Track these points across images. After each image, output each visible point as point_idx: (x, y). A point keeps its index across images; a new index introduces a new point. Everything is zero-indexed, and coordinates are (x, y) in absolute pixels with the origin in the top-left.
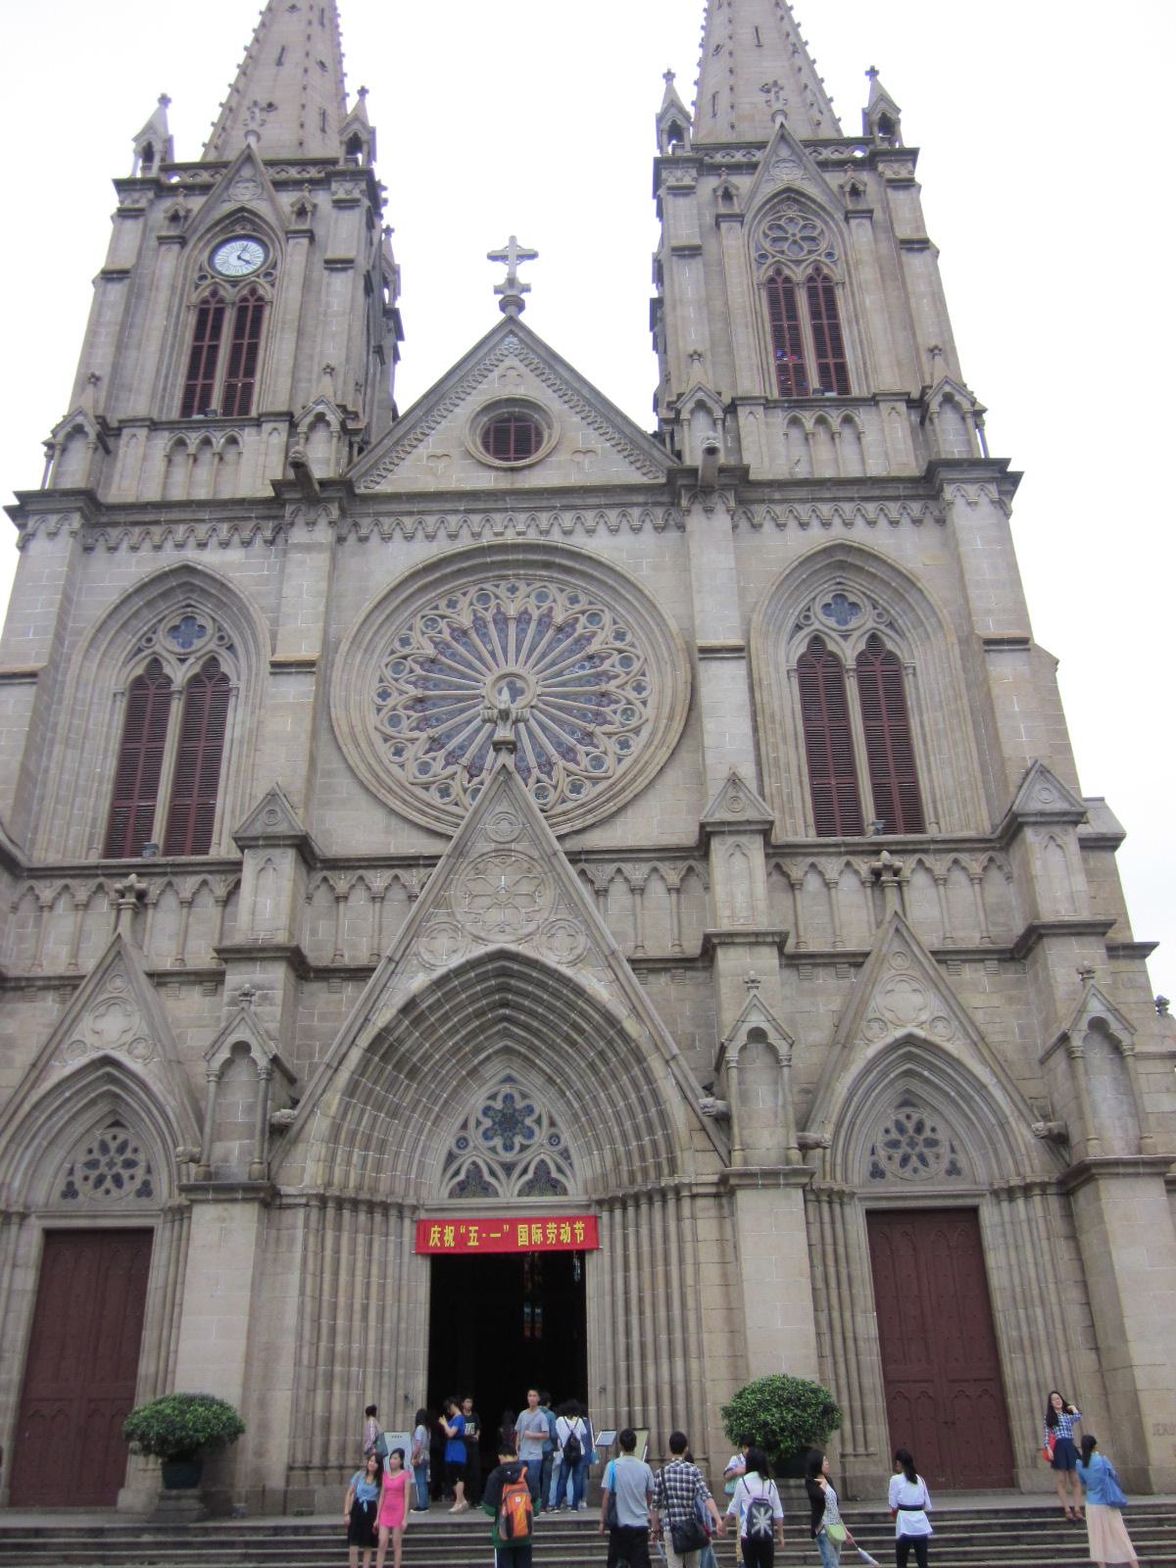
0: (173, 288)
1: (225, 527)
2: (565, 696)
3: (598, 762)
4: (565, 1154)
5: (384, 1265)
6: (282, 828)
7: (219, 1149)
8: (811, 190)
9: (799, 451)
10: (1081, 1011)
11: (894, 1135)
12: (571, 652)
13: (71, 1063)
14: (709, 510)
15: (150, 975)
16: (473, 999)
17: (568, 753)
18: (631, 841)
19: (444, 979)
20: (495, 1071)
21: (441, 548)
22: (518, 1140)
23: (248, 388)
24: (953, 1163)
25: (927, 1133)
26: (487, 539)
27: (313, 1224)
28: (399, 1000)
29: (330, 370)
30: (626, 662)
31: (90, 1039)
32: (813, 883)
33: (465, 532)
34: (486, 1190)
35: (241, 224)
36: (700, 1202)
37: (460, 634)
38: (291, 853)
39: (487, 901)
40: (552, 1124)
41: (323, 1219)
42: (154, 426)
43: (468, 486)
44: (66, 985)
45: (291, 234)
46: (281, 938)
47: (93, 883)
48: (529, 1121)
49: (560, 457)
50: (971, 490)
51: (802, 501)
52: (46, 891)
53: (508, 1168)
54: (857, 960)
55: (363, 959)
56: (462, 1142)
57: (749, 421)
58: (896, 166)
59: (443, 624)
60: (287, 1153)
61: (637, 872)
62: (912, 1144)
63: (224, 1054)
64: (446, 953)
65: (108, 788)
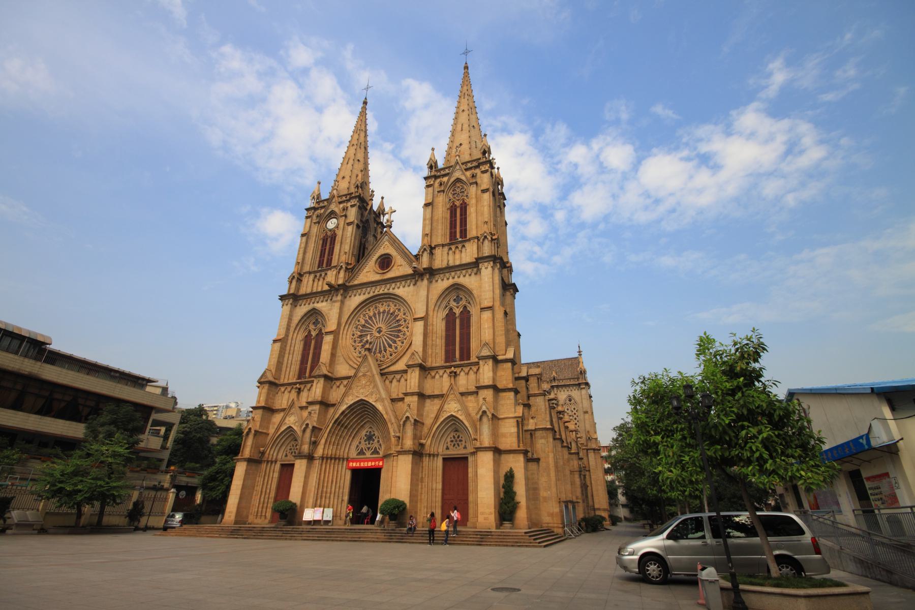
0: (316, 235)
1: (322, 297)
2: (390, 331)
3: (396, 348)
4: (380, 445)
5: (337, 471)
6: (321, 373)
7: (303, 447)
8: (463, 178)
9: (451, 257)
10: (480, 409)
11: (453, 439)
13: (283, 428)
14: (422, 280)
15: (300, 407)
16: (359, 410)
17: (390, 346)
18: (399, 369)
20: (368, 425)
21: (367, 296)
22: (371, 442)
23: (332, 258)
24: (465, 446)
25: (460, 438)
26: (376, 293)
27: (320, 463)
28: (340, 412)
29: (346, 253)
30: (405, 321)
31: (288, 423)
32: (437, 376)
33: (371, 292)
34: (364, 454)
35: (332, 214)
36: (395, 458)
37: (370, 318)
38: (323, 379)
39: (360, 387)
41: (322, 462)
42: (310, 273)
43: (373, 280)
44: (283, 410)
45: (342, 216)
46: (320, 399)
47: (291, 387)
49: (395, 268)
50: (486, 264)
51: (448, 272)
52: (283, 389)
53: (369, 448)
54: (442, 396)
56: (360, 443)
57: (438, 252)
59: (367, 315)
60: (316, 448)
61: (398, 376)
62: (456, 441)
63: (304, 426)
64: (350, 400)
65: (299, 363)
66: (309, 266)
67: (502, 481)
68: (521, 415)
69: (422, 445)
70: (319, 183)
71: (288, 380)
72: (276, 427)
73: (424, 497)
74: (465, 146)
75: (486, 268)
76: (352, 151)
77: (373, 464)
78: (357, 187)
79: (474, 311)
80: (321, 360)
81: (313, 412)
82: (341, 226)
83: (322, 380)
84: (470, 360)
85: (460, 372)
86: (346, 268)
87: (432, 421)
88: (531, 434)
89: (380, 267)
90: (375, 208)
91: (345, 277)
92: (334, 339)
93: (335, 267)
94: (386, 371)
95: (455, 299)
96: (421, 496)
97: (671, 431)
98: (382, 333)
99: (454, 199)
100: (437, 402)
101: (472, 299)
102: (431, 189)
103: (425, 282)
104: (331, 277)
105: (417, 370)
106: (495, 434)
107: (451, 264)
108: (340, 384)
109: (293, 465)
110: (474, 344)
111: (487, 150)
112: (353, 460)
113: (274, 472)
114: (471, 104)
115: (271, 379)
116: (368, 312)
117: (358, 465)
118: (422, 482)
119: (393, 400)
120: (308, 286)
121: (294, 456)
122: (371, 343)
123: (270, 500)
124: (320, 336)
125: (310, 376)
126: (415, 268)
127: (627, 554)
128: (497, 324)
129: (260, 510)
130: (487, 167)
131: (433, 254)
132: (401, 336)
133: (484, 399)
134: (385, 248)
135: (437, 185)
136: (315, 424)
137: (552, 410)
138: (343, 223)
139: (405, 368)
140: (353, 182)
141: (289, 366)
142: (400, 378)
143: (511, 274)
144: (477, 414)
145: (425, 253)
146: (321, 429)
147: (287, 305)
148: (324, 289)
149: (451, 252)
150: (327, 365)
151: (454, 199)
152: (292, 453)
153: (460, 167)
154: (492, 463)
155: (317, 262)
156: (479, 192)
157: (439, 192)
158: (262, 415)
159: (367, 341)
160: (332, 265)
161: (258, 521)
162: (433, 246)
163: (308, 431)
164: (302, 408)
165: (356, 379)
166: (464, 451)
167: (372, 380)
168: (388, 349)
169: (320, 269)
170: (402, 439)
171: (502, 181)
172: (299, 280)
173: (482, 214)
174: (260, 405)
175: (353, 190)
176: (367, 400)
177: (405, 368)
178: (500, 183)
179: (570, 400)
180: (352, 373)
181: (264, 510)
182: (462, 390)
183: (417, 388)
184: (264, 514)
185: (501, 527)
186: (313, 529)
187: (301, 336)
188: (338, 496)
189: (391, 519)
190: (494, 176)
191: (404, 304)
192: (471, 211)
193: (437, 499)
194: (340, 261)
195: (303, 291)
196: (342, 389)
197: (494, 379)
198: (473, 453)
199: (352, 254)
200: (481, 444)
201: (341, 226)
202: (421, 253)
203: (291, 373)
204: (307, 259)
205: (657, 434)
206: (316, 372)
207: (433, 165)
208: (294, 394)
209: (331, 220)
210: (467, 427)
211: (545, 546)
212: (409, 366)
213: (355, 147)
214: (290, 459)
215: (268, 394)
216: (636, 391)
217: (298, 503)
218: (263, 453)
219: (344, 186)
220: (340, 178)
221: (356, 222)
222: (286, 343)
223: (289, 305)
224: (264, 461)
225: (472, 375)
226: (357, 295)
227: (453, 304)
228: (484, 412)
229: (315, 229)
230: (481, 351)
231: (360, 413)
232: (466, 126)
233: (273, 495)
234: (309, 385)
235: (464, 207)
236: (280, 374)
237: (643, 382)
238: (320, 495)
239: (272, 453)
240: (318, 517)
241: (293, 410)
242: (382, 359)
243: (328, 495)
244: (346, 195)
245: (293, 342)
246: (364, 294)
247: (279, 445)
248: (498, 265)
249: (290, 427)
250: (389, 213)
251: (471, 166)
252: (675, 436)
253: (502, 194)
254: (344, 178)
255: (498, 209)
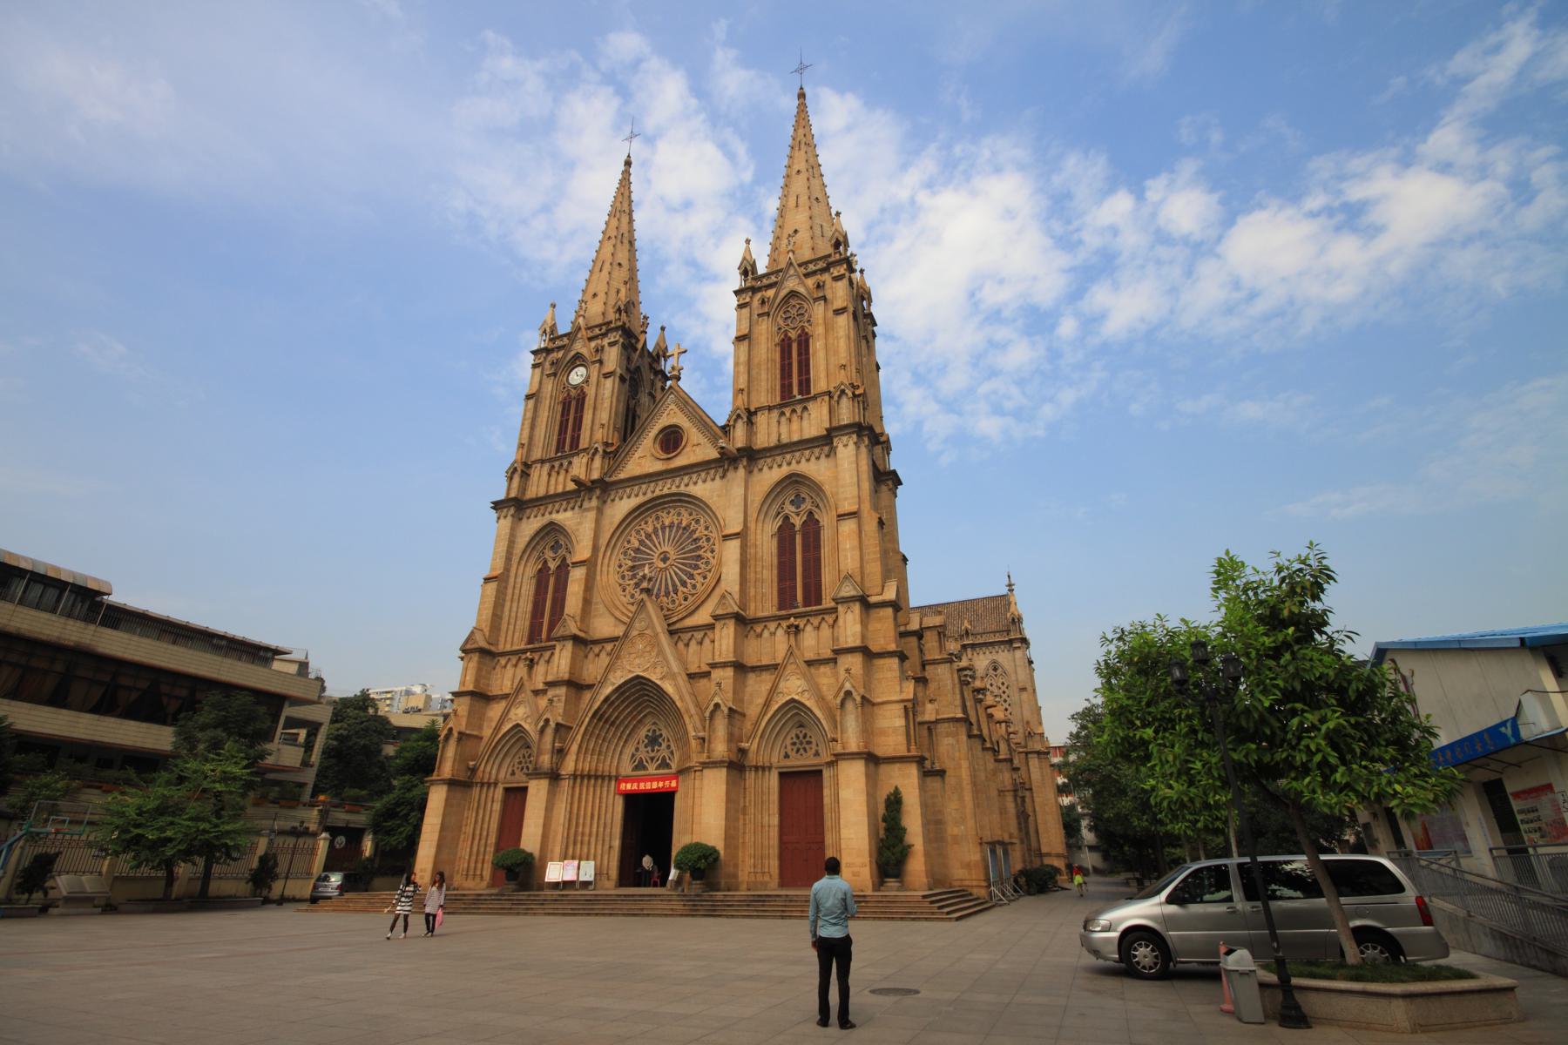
0: (551, 396)
2: (683, 559)
3: (694, 587)
4: (672, 753)
5: (601, 798)
6: (567, 633)
7: (541, 758)
8: (802, 290)
9: (784, 429)
12: (688, 538)
15: (533, 691)
16: (633, 694)
17: (684, 584)
18: (701, 622)
19: (620, 687)
20: (649, 720)
21: (641, 499)
22: (656, 748)
23: (579, 436)
25: (808, 739)
26: (658, 493)
28: (602, 698)
29: (603, 425)
30: (708, 540)
31: (514, 718)
32: (766, 634)
33: (649, 491)
34: (645, 768)
35: (578, 360)
36: (698, 773)
37: (648, 536)
38: (571, 642)
39: (633, 656)
40: (668, 741)
41: (574, 783)
42: (542, 461)
44: (505, 697)
46: (566, 677)
48: (660, 740)
49: (688, 449)
50: (845, 439)
52: (503, 661)
53: (652, 759)
54: (774, 667)
55: (591, 683)
56: (637, 749)
57: (761, 419)
58: (838, 268)
59: (642, 532)
61: (699, 635)
62: (801, 743)
63: (541, 723)
64: (618, 678)
65: (528, 616)
66: (540, 450)
67: (882, 810)
68: (911, 696)
69: (743, 752)
70: (554, 306)
71: (512, 645)
72: (494, 725)
73: (750, 838)
74: (804, 235)
75: (846, 446)
76: (609, 248)
77: (661, 784)
78: (619, 310)
79: (826, 520)
80: (567, 610)
81: (555, 699)
82: (594, 379)
83: (569, 645)
84: (821, 604)
85: (805, 625)
86: (604, 451)
87: (759, 710)
88: (929, 728)
89: (662, 450)
90: (651, 347)
91: (602, 468)
92: (587, 574)
93: (584, 450)
94: (678, 626)
95: (792, 501)
96: (744, 838)
97: (1171, 720)
98: (668, 563)
99: (787, 328)
100: (767, 679)
101: (821, 499)
102: (746, 311)
103: (741, 472)
104: (579, 467)
105: (731, 624)
106: (867, 730)
107: (785, 439)
108: (601, 651)
109: (525, 789)
110: (827, 577)
111: (841, 239)
112: (627, 779)
113: (493, 801)
114: (811, 160)
115: (483, 644)
116: (643, 526)
117: (635, 787)
118: (744, 814)
119: (691, 676)
120: (540, 483)
121: (527, 775)
122: (650, 580)
123: (488, 849)
124: (564, 569)
125: (549, 639)
126: (722, 448)
127: (1099, 929)
128: (866, 542)
129: (472, 865)
130: (842, 269)
131: (752, 423)
132: (703, 566)
133: (847, 670)
134: (670, 415)
135: (756, 302)
136: (560, 720)
137: (965, 687)
138: (596, 373)
139: (711, 621)
140: (612, 302)
141: (512, 621)
142: (702, 639)
143: (888, 454)
144: (836, 696)
145: (740, 421)
146: (571, 728)
147: (505, 517)
148: (568, 489)
149: (783, 419)
150: (578, 618)
151: (787, 328)
152: (522, 769)
153: (796, 271)
154: (863, 779)
155: (555, 443)
156: (830, 313)
157: (759, 315)
158: (471, 706)
159: (644, 577)
160: (581, 447)
161: (470, 884)
162: (753, 409)
163: (549, 732)
164: (536, 693)
165: (627, 640)
166: (816, 761)
167: (655, 643)
168: (681, 589)
169: (559, 454)
170: (710, 742)
171: (869, 294)
172: (525, 475)
173: (836, 352)
174: (465, 689)
175: (611, 316)
176: (647, 676)
177: (711, 621)
178: (866, 296)
179: (995, 669)
180: (619, 631)
181: (479, 865)
182: (810, 656)
183: (731, 655)
184: (478, 873)
185: (882, 888)
186: (563, 895)
187: (531, 570)
188: (603, 840)
189: (694, 877)
190: (855, 286)
191: (706, 512)
192: (817, 347)
193: (771, 842)
194: (594, 440)
195: (531, 493)
196: (604, 659)
197: (863, 637)
198: (831, 764)
199: (614, 427)
200: (844, 748)
201: (594, 379)
202: (732, 423)
203: (517, 635)
204: (536, 438)
205: (1144, 726)
206: (558, 632)
207: (749, 268)
208: (522, 670)
209: (576, 370)
210: (819, 720)
211: (958, 919)
212: (717, 618)
213: (613, 241)
214: (519, 779)
215: (479, 670)
216: (1109, 652)
217: (536, 854)
218: (474, 770)
219: (595, 309)
220: (588, 297)
221: (619, 371)
222: (507, 581)
223: (509, 519)
224: (477, 783)
225: (826, 631)
226: (625, 497)
227: (789, 509)
228: (848, 693)
229: (549, 386)
230: (839, 590)
231: (638, 699)
232: (803, 199)
233: (494, 841)
234: (547, 654)
235: (804, 341)
236: (498, 636)
237: (1120, 639)
238: (572, 838)
239: (488, 769)
240: (570, 876)
241: (521, 697)
242: (671, 606)
243: (586, 839)
244: (599, 326)
245: (519, 580)
246: (637, 496)
247: (501, 756)
248: (866, 439)
249: (518, 725)
250: (676, 356)
251: (814, 268)
252: (1177, 727)
253: (870, 316)
254: (595, 295)
255: (864, 342)
